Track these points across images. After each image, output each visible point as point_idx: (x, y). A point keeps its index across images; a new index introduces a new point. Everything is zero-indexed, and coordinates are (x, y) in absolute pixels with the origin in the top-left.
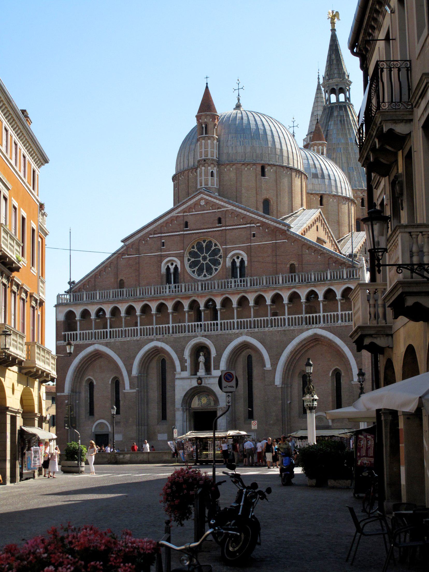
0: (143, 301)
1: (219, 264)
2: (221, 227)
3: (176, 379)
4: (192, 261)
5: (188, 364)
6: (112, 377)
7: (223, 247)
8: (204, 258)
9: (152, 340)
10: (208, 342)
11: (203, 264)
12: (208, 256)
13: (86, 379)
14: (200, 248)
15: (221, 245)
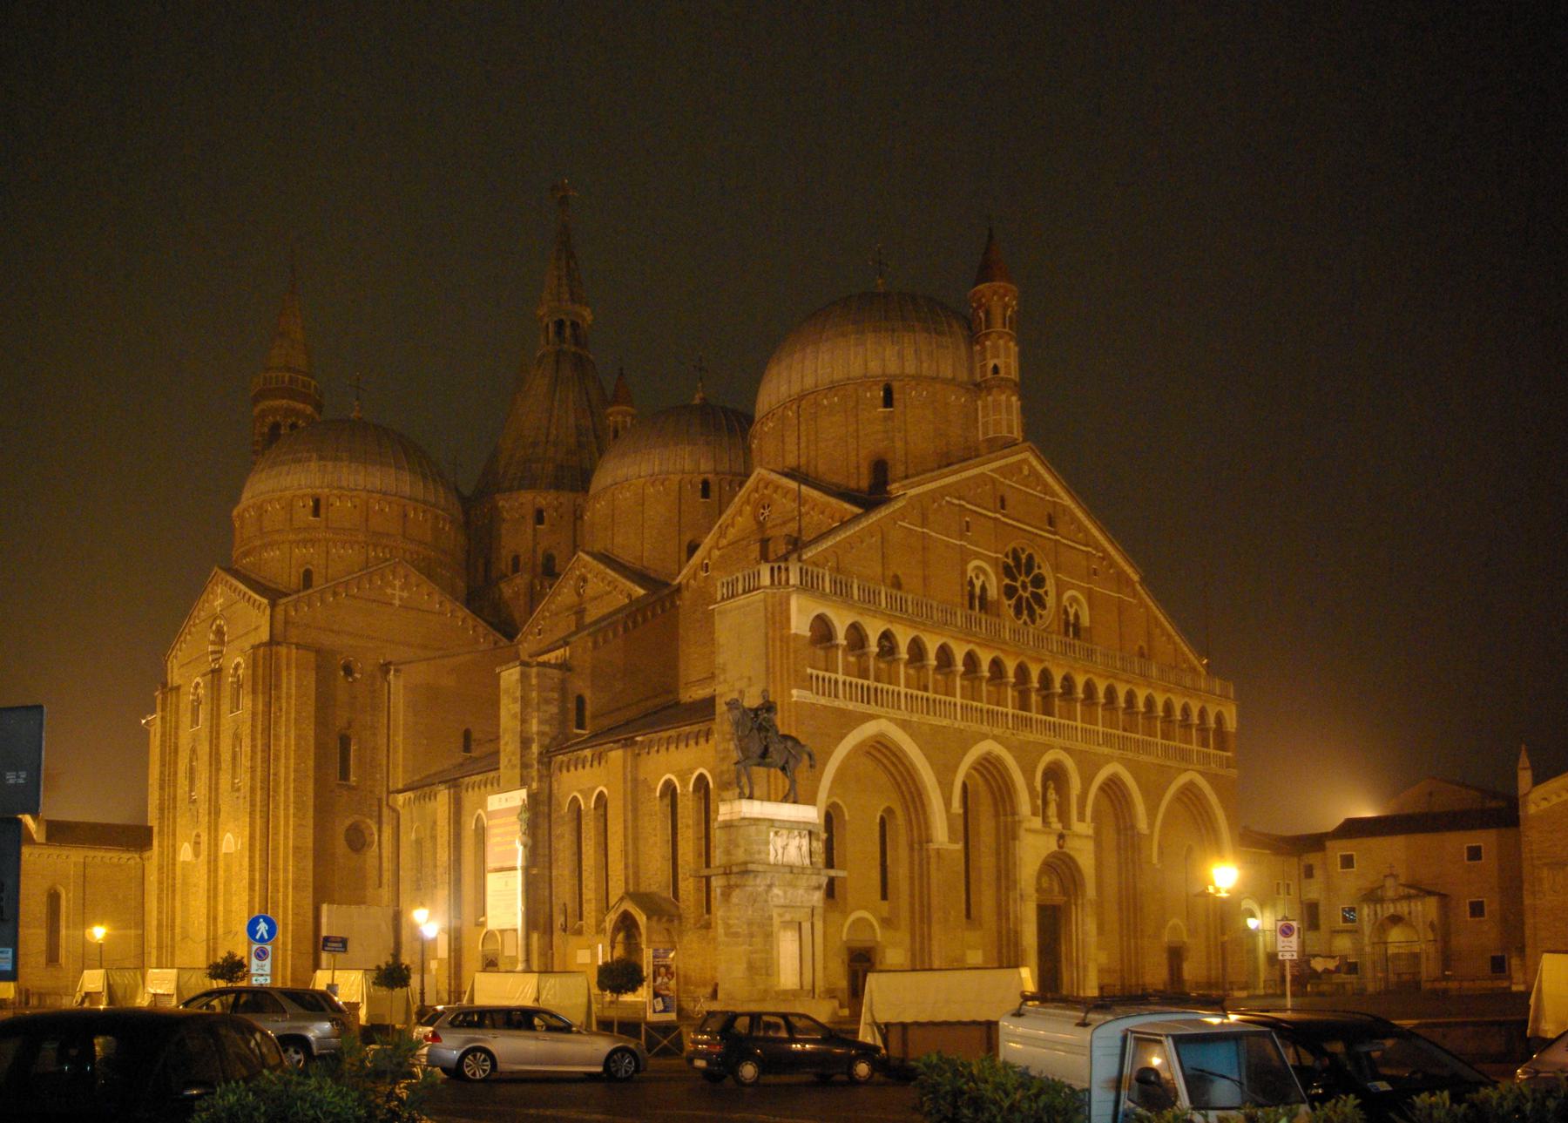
0: (970, 642)
1: (1043, 606)
2: (1055, 533)
3: (1026, 830)
4: (1007, 585)
5: (1039, 802)
6: (882, 808)
7: (1059, 575)
8: (1024, 587)
9: (985, 737)
10: (1070, 764)
11: (1020, 598)
12: (1029, 585)
13: (832, 800)
14: (1016, 558)
15: (1057, 568)
